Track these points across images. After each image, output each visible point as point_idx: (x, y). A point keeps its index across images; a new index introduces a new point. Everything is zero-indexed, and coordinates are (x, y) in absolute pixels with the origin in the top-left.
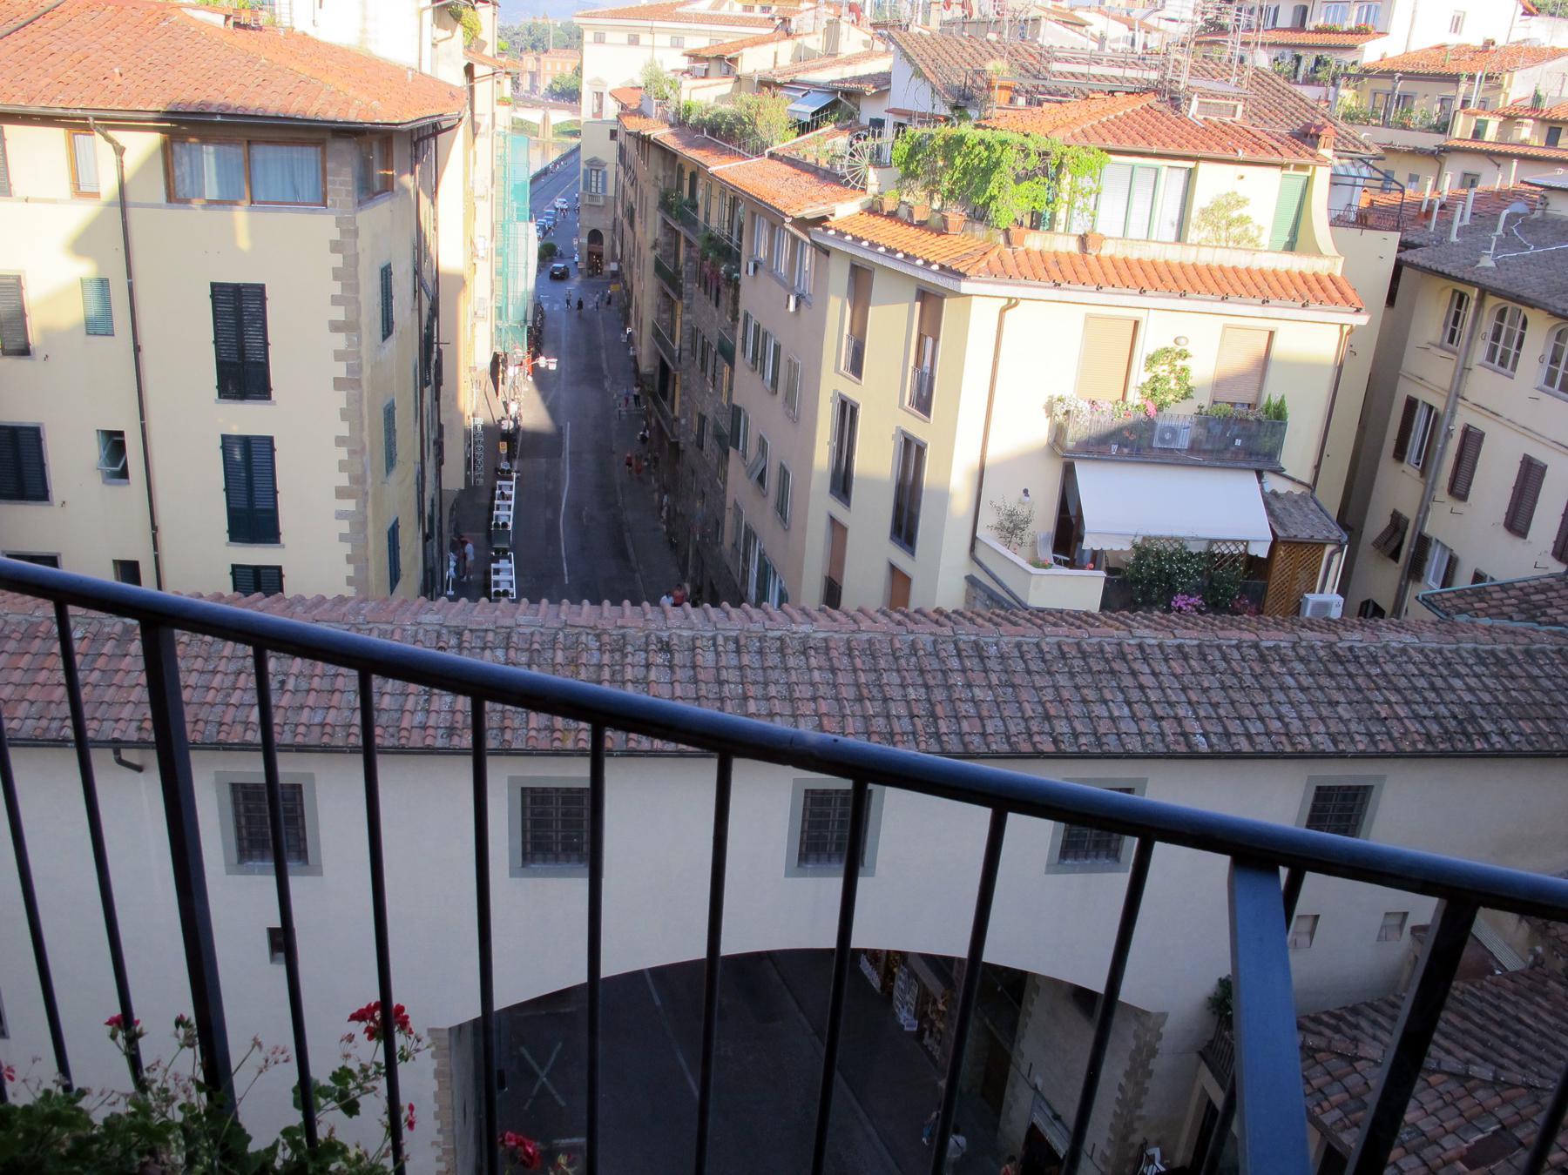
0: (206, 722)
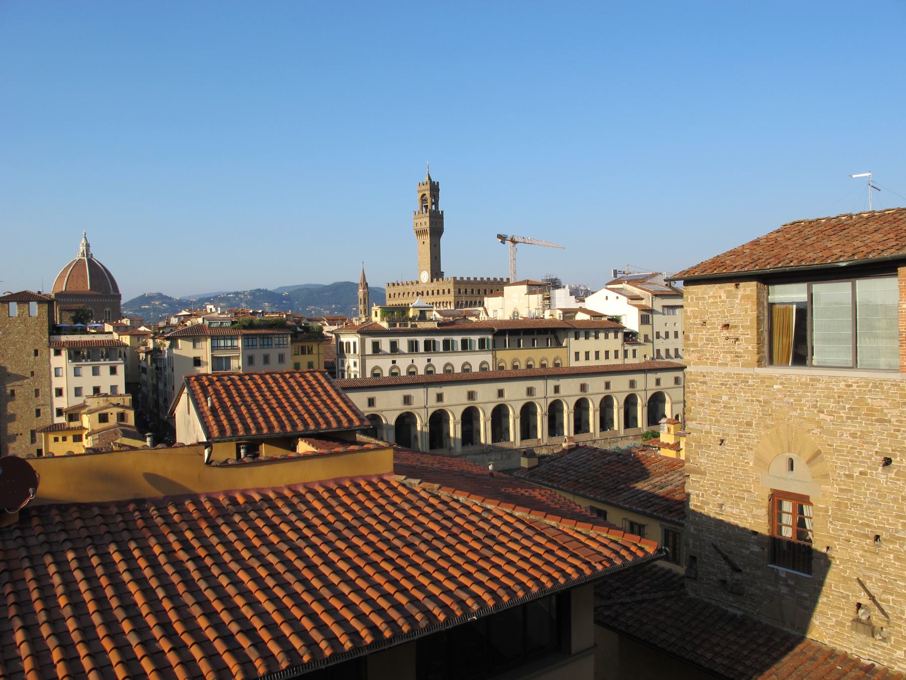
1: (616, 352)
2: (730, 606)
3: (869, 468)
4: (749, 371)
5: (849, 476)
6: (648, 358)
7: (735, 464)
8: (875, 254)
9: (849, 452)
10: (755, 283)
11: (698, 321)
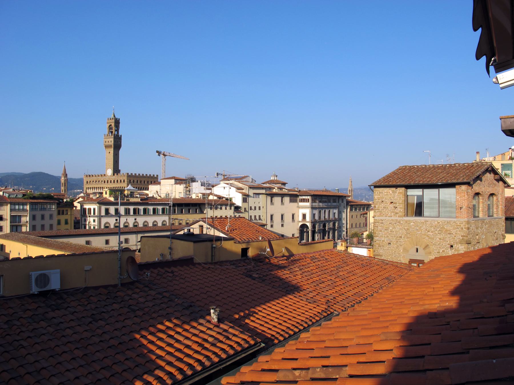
4: (401, 218)
5: (439, 252)
11: (380, 201)
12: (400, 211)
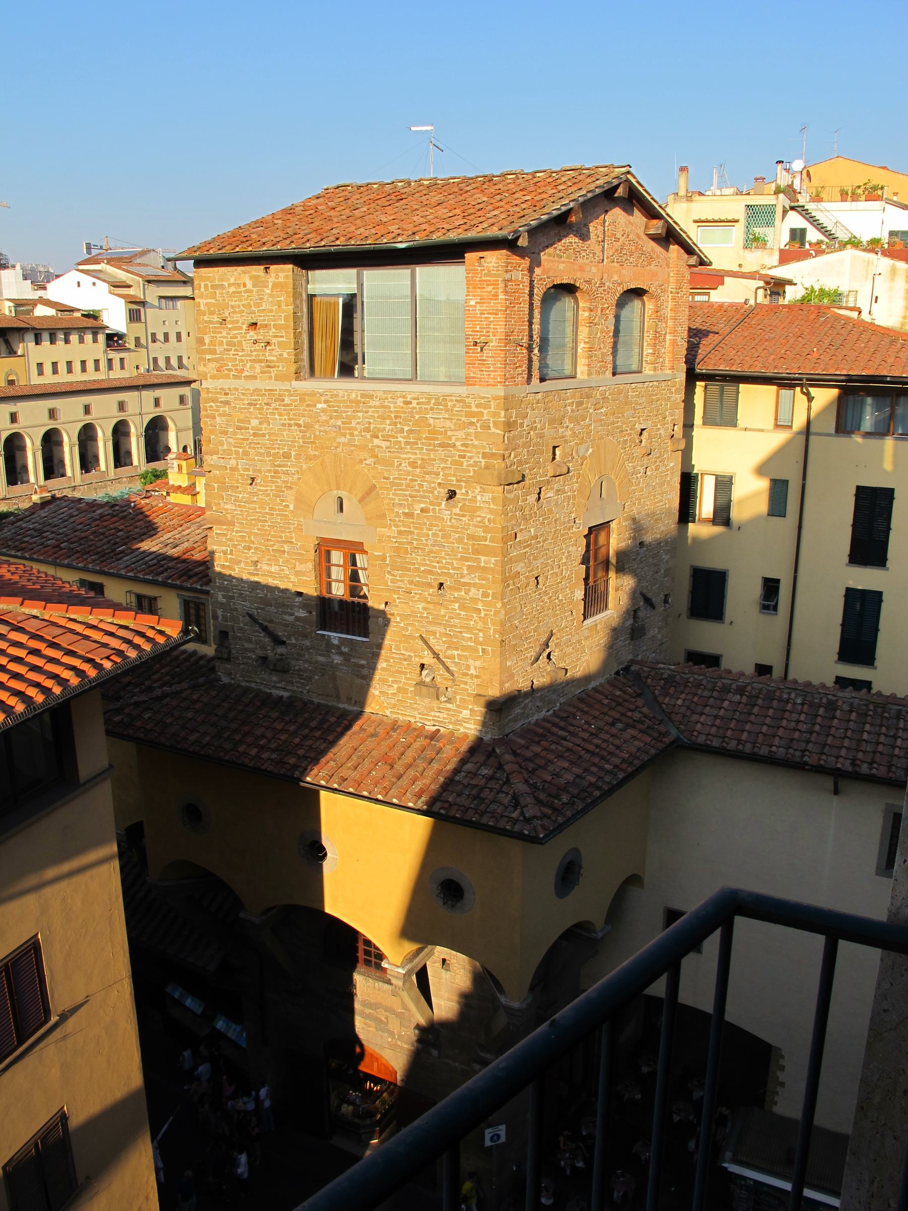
0: (897, 767)
1: (97, 362)
2: (274, 687)
3: (432, 503)
4: (285, 386)
5: (409, 515)
6: (142, 370)
7: (270, 509)
8: (439, 234)
9: (408, 486)
10: (290, 267)
11: (215, 318)
12: (280, 358)
